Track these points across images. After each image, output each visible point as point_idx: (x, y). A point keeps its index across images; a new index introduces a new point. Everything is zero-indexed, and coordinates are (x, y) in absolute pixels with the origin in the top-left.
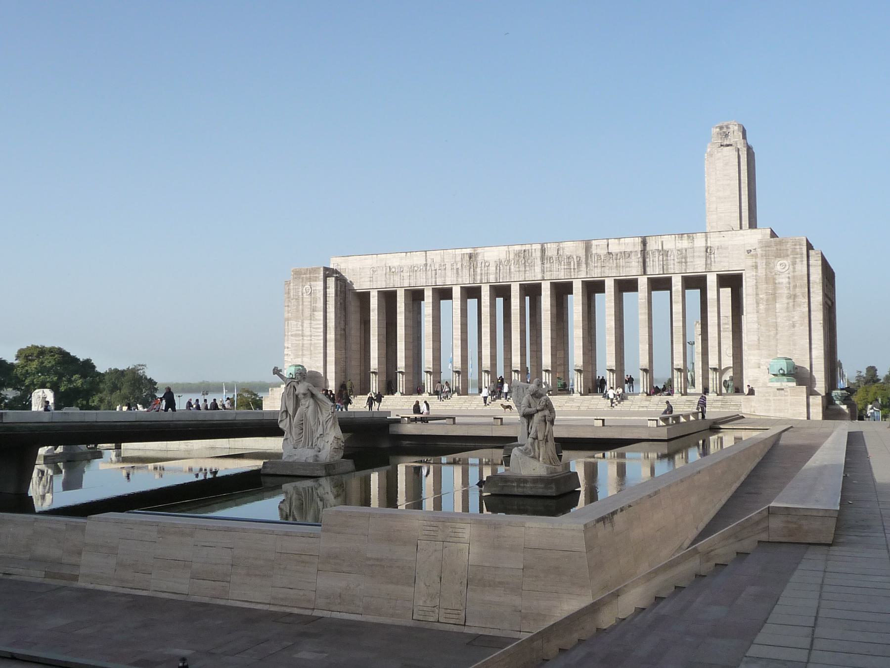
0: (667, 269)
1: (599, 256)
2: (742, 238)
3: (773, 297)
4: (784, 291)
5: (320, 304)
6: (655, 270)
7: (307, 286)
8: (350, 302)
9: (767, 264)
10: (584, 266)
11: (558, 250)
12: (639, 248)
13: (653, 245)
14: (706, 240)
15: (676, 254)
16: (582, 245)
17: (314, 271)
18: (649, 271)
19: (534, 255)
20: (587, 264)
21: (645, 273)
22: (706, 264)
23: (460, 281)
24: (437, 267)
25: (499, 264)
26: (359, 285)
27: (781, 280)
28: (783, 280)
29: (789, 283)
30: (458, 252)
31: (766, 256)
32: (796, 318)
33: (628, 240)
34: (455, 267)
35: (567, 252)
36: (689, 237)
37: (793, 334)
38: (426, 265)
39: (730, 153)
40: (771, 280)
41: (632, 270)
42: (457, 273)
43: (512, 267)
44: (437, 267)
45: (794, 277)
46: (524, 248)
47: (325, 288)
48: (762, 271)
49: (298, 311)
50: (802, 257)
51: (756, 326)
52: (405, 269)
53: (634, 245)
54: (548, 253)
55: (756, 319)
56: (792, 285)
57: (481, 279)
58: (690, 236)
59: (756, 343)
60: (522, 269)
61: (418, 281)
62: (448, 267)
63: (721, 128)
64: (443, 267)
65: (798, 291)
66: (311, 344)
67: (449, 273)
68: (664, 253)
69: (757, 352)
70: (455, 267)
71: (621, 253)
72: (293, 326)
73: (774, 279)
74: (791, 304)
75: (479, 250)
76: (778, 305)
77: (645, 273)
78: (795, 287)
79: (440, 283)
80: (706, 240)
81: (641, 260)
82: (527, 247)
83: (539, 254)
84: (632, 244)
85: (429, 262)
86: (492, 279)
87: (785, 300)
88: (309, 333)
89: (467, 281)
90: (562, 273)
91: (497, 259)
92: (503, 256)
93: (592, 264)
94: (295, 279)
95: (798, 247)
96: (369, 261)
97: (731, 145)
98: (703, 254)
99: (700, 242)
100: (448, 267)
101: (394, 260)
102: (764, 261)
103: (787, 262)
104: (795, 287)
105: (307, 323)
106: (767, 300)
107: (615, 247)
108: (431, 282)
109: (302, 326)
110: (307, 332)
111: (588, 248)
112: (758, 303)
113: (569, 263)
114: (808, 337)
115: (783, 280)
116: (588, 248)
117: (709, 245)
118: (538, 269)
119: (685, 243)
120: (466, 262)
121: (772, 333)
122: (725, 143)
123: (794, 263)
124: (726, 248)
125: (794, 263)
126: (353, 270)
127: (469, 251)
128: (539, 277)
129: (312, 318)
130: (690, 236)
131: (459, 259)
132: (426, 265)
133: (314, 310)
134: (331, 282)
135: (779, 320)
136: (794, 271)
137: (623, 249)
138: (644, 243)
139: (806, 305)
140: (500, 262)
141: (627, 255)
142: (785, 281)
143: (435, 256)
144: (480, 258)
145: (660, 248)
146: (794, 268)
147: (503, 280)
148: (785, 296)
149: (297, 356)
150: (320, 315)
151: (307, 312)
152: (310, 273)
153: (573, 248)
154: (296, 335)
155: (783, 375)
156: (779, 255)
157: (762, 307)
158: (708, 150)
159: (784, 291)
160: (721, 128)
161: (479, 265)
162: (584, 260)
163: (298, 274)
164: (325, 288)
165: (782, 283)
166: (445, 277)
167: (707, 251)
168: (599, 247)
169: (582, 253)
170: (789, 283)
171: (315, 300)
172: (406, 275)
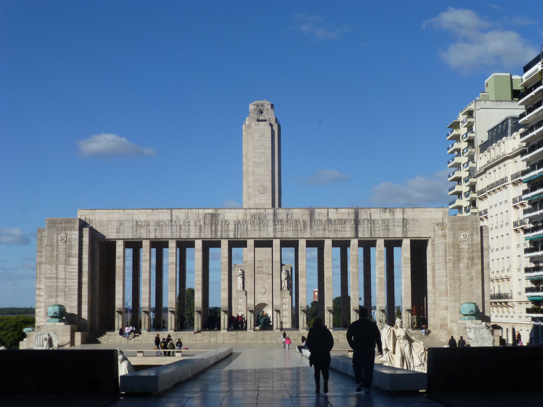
0: (374, 234)
1: (321, 221)
2: (429, 214)
3: (458, 259)
4: (465, 255)
5: (76, 251)
6: (364, 234)
7: (63, 235)
8: (102, 252)
9: (454, 234)
10: (309, 228)
11: (288, 215)
12: (352, 217)
13: (363, 215)
14: (403, 214)
15: (381, 223)
16: (307, 212)
17: (69, 221)
18: (360, 235)
19: (267, 218)
20: (311, 227)
21: (357, 237)
22: (403, 232)
23: (203, 236)
24: (182, 223)
25: (237, 223)
26: (110, 234)
27: (463, 247)
28: (465, 246)
29: (469, 249)
30: (201, 211)
31: (452, 229)
32: (474, 274)
33: (343, 210)
34: (198, 224)
35: (295, 217)
36: (390, 211)
37: (471, 286)
38: (171, 221)
39: (265, 127)
40: (456, 246)
41: (347, 233)
42: (200, 229)
43: (249, 226)
44: (182, 223)
45: (472, 244)
46: (259, 211)
47: (81, 236)
48: (449, 240)
49: (52, 256)
50: (477, 231)
51: (444, 279)
52: (152, 223)
53: (349, 214)
54: (280, 217)
55: (445, 274)
56: (470, 250)
57: (221, 235)
58: (392, 211)
59: (445, 291)
60: (257, 228)
61: (165, 234)
62: (192, 223)
63: (257, 106)
64: (187, 223)
65: (475, 255)
66: (65, 286)
67: (192, 229)
68: (371, 221)
69: (445, 298)
70: (198, 224)
71: (339, 220)
72: (46, 269)
73: (459, 245)
74: (470, 264)
75: (220, 211)
76: (461, 265)
77: (357, 237)
78: (473, 251)
79: (184, 236)
80: (403, 214)
81: (354, 226)
82: (262, 211)
83: (271, 217)
84: (346, 213)
85: (174, 218)
86: (231, 235)
87: (466, 261)
88: (63, 277)
89: (208, 235)
90: (291, 234)
91: (235, 219)
92: (241, 217)
93: (315, 227)
94: (49, 227)
95: (474, 223)
96: (116, 215)
97: (265, 121)
98: (401, 224)
99: (399, 215)
100: (192, 223)
101: (141, 215)
102: (452, 232)
103: (467, 233)
104: (473, 251)
105: (61, 267)
106: (454, 260)
107: (333, 215)
108: (176, 235)
109: (57, 270)
110: (61, 275)
111: (312, 215)
112: (446, 263)
113: (296, 226)
114: (481, 288)
115: (465, 246)
116: (312, 215)
117: (405, 217)
118: (271, 229)
119: (387, 215)
120: (208, 221)
121: (457, 284)
122: (261, 118)
123: (472, 235)
124: (418, 221)
125: (472, 235)
126: (100, 222)
127: (211, 211)
128: (271, 235)
129: (66, 263)
130: (392, 211)
131: (201, 217)
132: (171, 221)
133: (69, 256)
134: (86, 232)
135: (462, 275)
136: (472, 240)
137: (340, 216)
138: (357, 215)
139: (480, 265)
140: (239, 222)
141: (343, 222)
142: (466, 247)
143: (180, 214)
144: (221, 218)
145: (369, 218)
146: (472, 238)
147: (241, 236)
148: (466, 257)
149: (50, 297)
150: (75, 261)
151: (62, 258)
152: (66, 223)
153: (299, 214)
154: (50, 278)
155: (472, 315)
156: (461, 229)
157: (450, 265)
158: (247, 123)
159: (465, 255)
160: (257, 106)
161: (220, 223)
162: (309, 224)
163: (53, 223)
164: (81, 236)
165: (464, 249)
166: (189, 231)
167: (403, 222)
168: (320, 214)
169: (307, 218)
170: (469, 249)
171: (71, 247)
172: (152, 228)
